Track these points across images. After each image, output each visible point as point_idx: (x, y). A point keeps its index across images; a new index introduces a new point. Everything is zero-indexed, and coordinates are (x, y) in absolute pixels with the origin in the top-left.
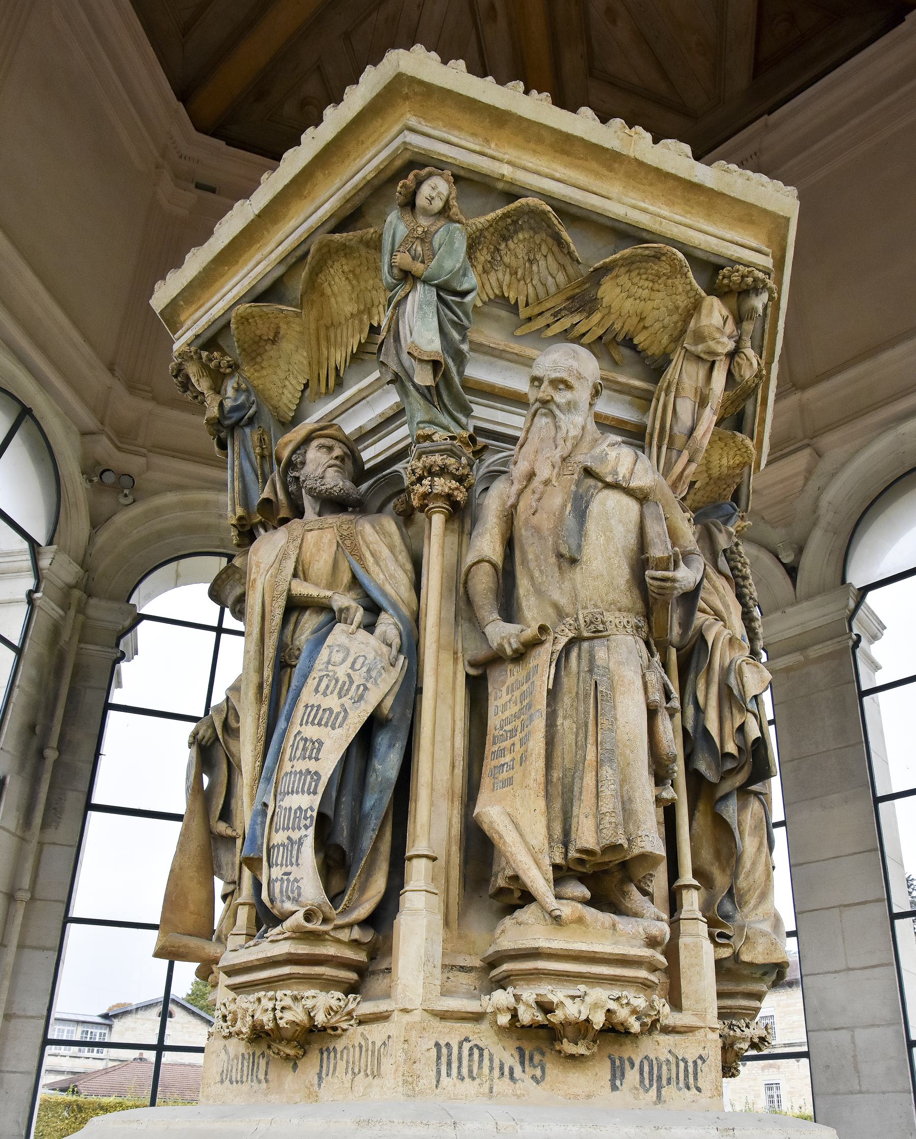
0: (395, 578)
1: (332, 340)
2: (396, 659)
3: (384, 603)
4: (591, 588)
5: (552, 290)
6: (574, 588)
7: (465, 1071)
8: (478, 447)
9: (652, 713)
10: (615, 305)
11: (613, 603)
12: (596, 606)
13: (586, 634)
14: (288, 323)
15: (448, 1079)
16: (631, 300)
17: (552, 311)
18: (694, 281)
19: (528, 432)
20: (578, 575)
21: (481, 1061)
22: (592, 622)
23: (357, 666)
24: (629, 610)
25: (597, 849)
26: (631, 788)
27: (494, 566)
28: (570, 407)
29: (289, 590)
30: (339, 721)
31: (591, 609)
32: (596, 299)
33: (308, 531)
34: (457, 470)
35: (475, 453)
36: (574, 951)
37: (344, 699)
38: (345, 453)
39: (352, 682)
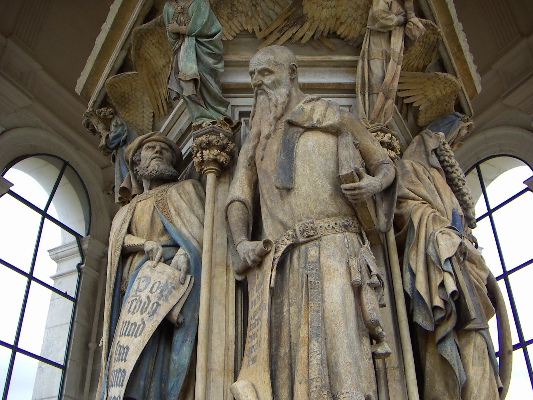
0: (190, 221)
1: (159, 83)
2: (185, 279)
3: (180, 242)
4: (302, 206)
5: (274, 17)
6: (291, 208)
8: (235, 124)
9: (357, 290)
11: (321, 213)
12: (308, 218)
13: (301, 240)
14: (135, 81)
16: (325, 10)
17: (278, 30)
19: (255, 107)
22: (304, 231)
23: (154, 290)
24: (334, 215)
26: (337, 354)
27: (242, 202)
28: (276, 84)
29: (124, 243)
30: (139, 331)
31: (305, 221)
32: (303, 15)
33: (139, 202)
34: (218, 142)
35: (233, 129)
37: (144, 315)
38: (162, 148)
39: (149, 301)
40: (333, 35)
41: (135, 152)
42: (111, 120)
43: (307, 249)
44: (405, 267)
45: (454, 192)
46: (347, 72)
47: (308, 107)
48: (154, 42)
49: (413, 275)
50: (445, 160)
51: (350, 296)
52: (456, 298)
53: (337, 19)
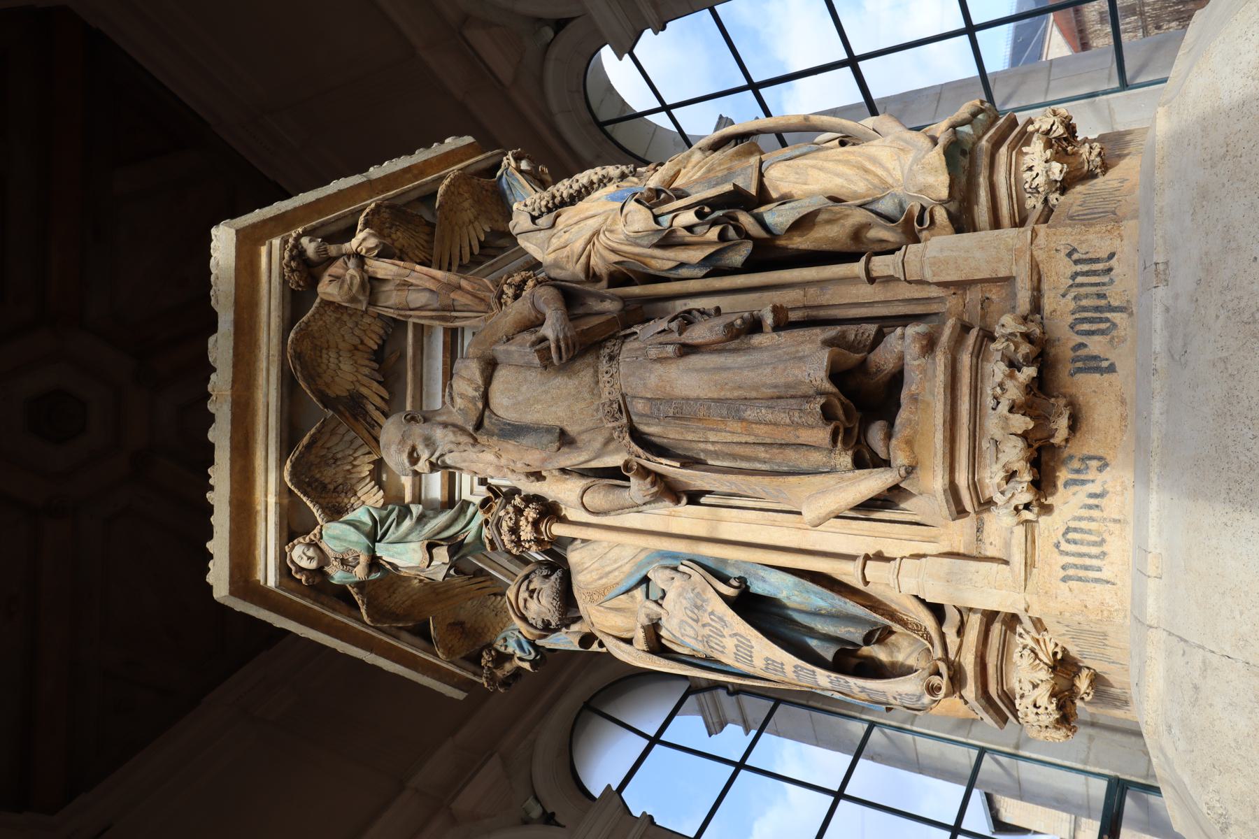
6: (586, 431)
7: (1094, 550)
9: (687, 350)
10: (351, 378)
11: (592, 392)
12: (597, 410)
13: (625, 420)
15: (1104, 570)
16: (342, 366)
18: (309, 314)
20: (572, 429)
21: (1082, 531)
25: (829, 429)
27: (584, 492)
28: (429, 442)
31: (600, 415)
35: (497, 496)
36: (944, 447)
40: (378, 356)
41: (531, 625)
42: (497, 651)
43: (637, 414)
44: (672, 274)
45: (589, 193)
46: (430, 337)
47: (458, 401)
48: (386, 595)
49: (682, 265)
50: (546, 206)
51: (695, 360)
52: (707, 210)
53: (356, 348)
